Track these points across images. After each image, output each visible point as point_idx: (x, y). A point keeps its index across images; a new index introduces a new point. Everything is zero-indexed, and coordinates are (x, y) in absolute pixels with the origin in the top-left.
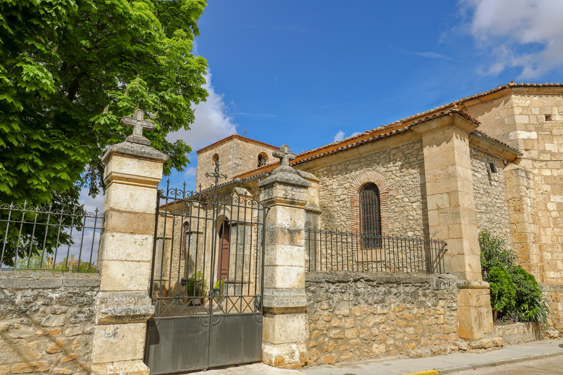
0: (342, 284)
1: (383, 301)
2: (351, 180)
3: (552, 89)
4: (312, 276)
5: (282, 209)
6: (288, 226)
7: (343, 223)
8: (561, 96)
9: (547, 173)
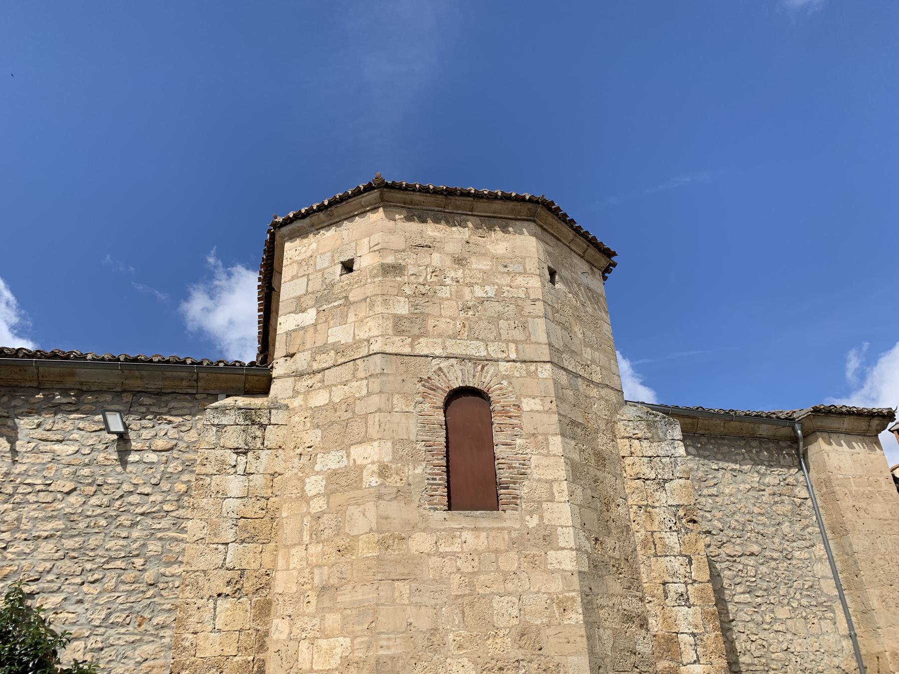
3: (354, 202)
8: (381, 209)
9: (320, 399)
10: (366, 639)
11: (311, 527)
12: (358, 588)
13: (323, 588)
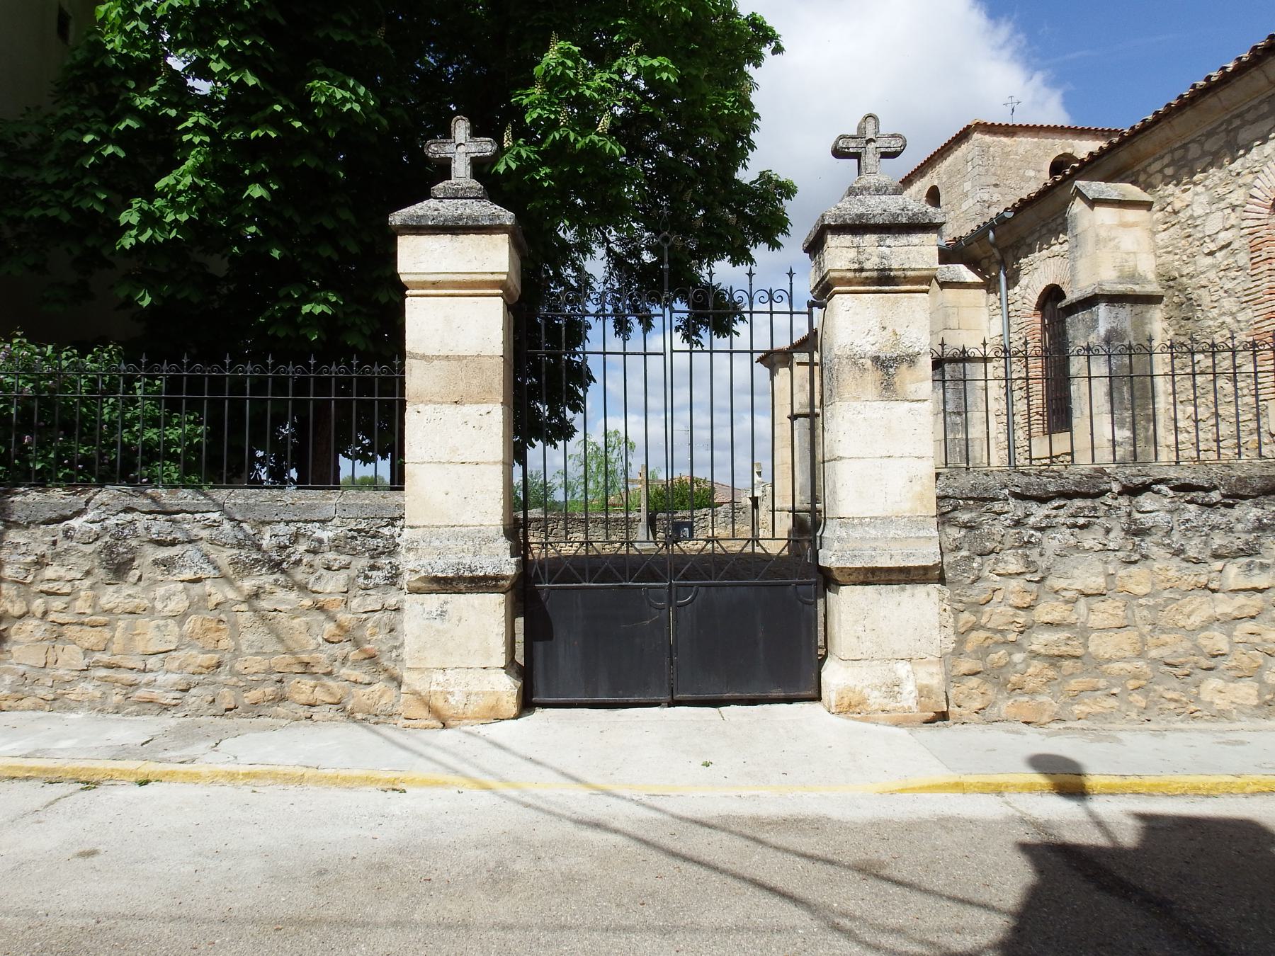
0: (1078, 503)
1: (1250, 551)
2: (1249, 179)
5: (850, 304)
6: (874, 348)
7: (1229, 320)
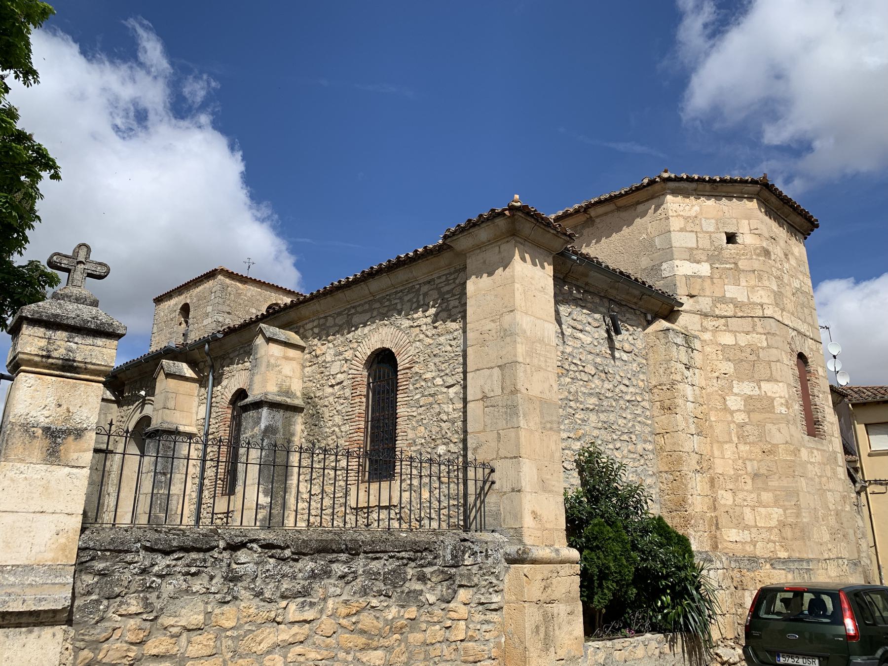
0: (194, 555)
1: (305, 593)
2: (355, 345)
3: (738, 187)
4: (93, 539)
5: (32, 382)
6: (47, 420)
7: (337, 429)
8: (755, 200)
9: (727, 339)
10: (795, 511)
11: (738, 432)
12: (783, 478)
13: (755, 474)
